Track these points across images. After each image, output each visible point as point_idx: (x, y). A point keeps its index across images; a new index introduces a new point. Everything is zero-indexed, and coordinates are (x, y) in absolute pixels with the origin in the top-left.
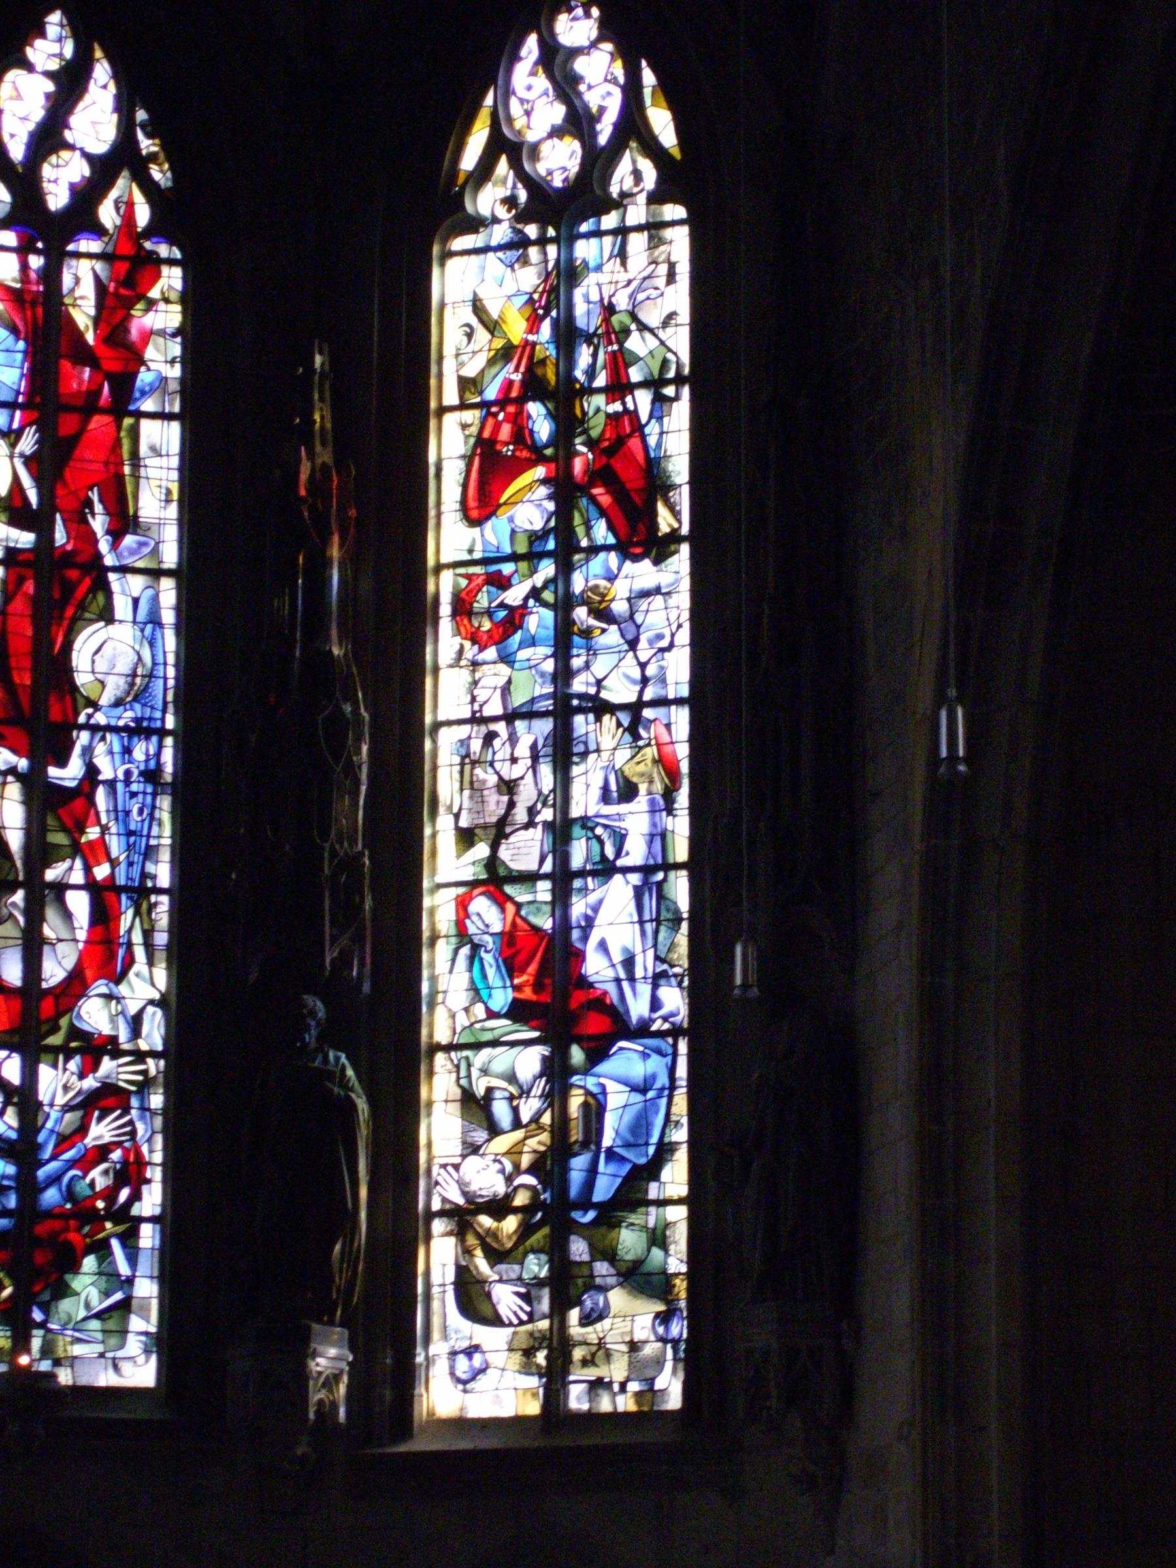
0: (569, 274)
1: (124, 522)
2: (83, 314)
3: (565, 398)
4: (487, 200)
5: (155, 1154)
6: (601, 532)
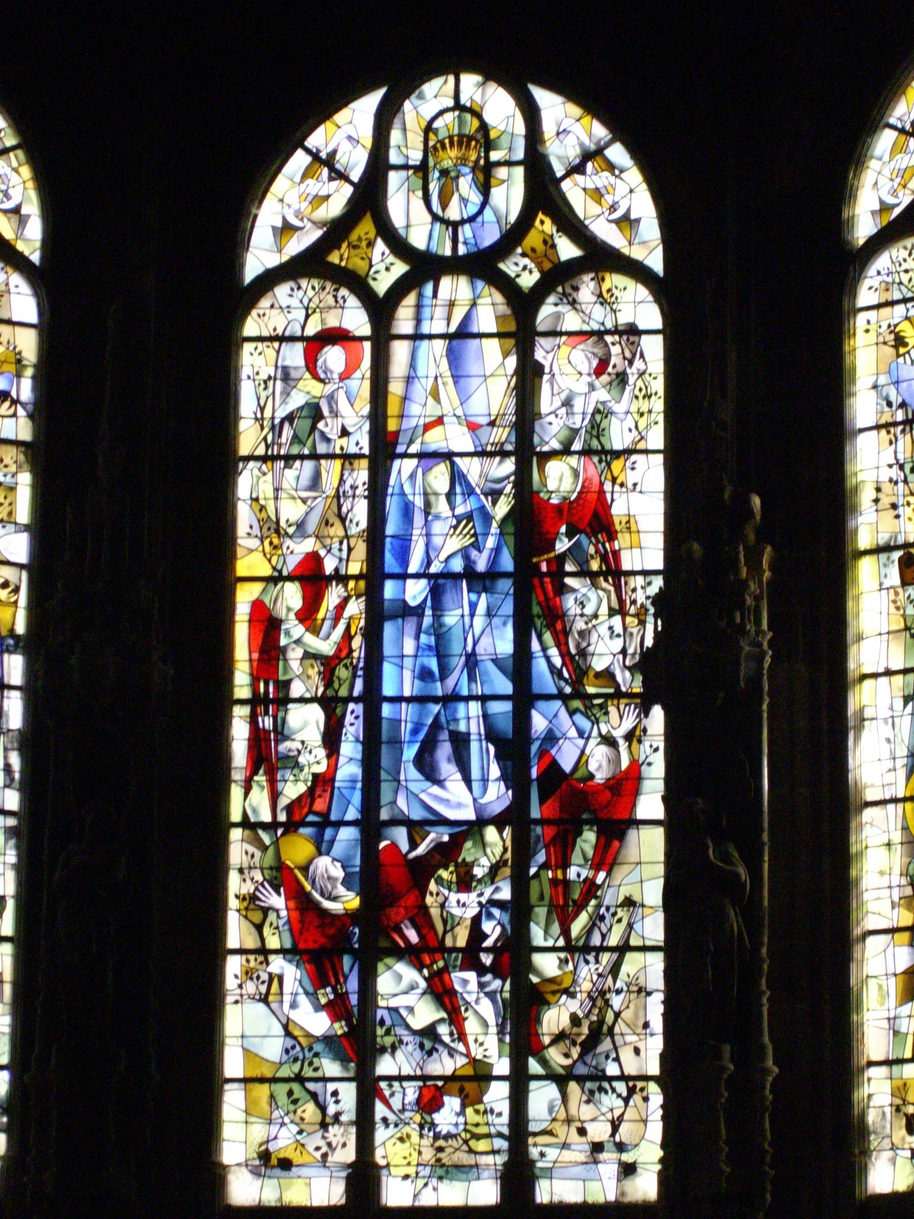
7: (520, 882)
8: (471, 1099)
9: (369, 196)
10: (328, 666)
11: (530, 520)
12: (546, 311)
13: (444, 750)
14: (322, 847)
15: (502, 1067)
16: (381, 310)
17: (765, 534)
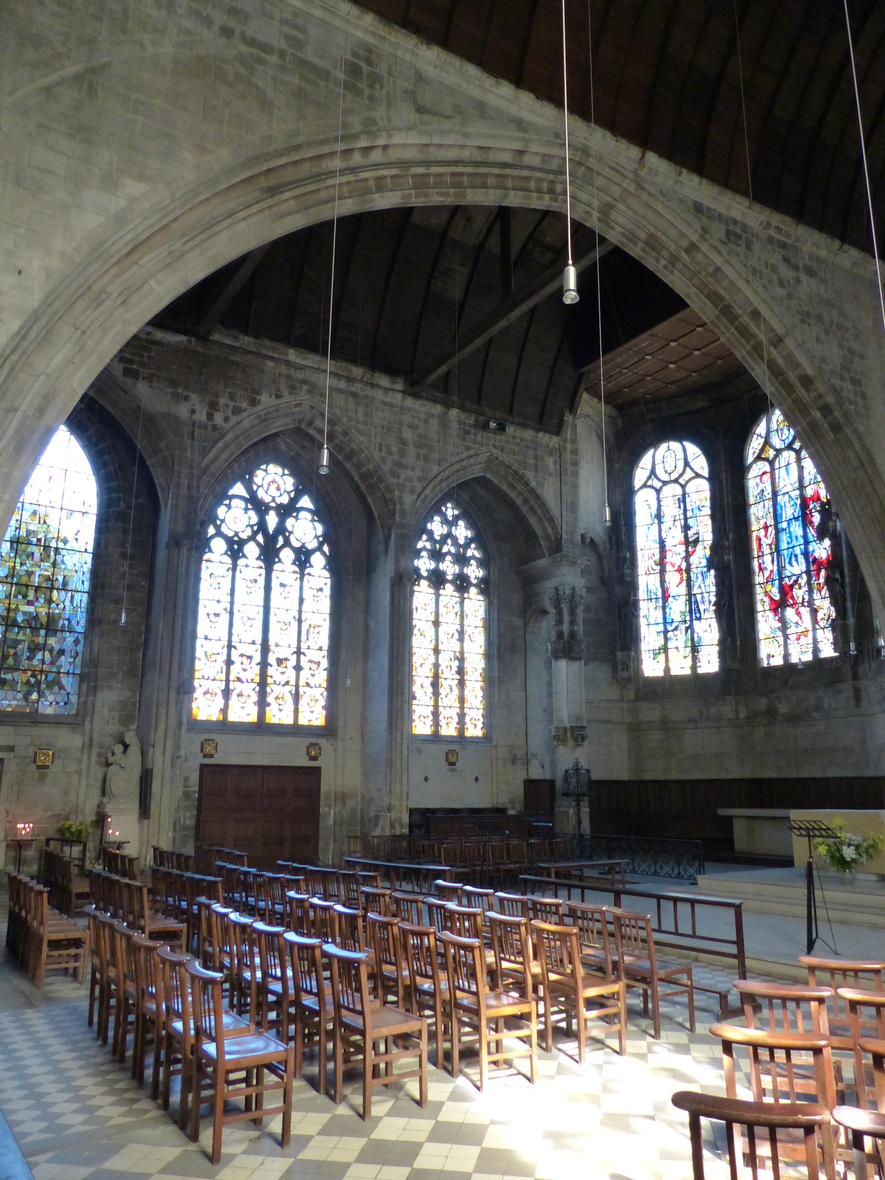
8: (806, 636)
10: (770, 545)
14: (773, 585)
15: (810, 628)
16: (772, 463)
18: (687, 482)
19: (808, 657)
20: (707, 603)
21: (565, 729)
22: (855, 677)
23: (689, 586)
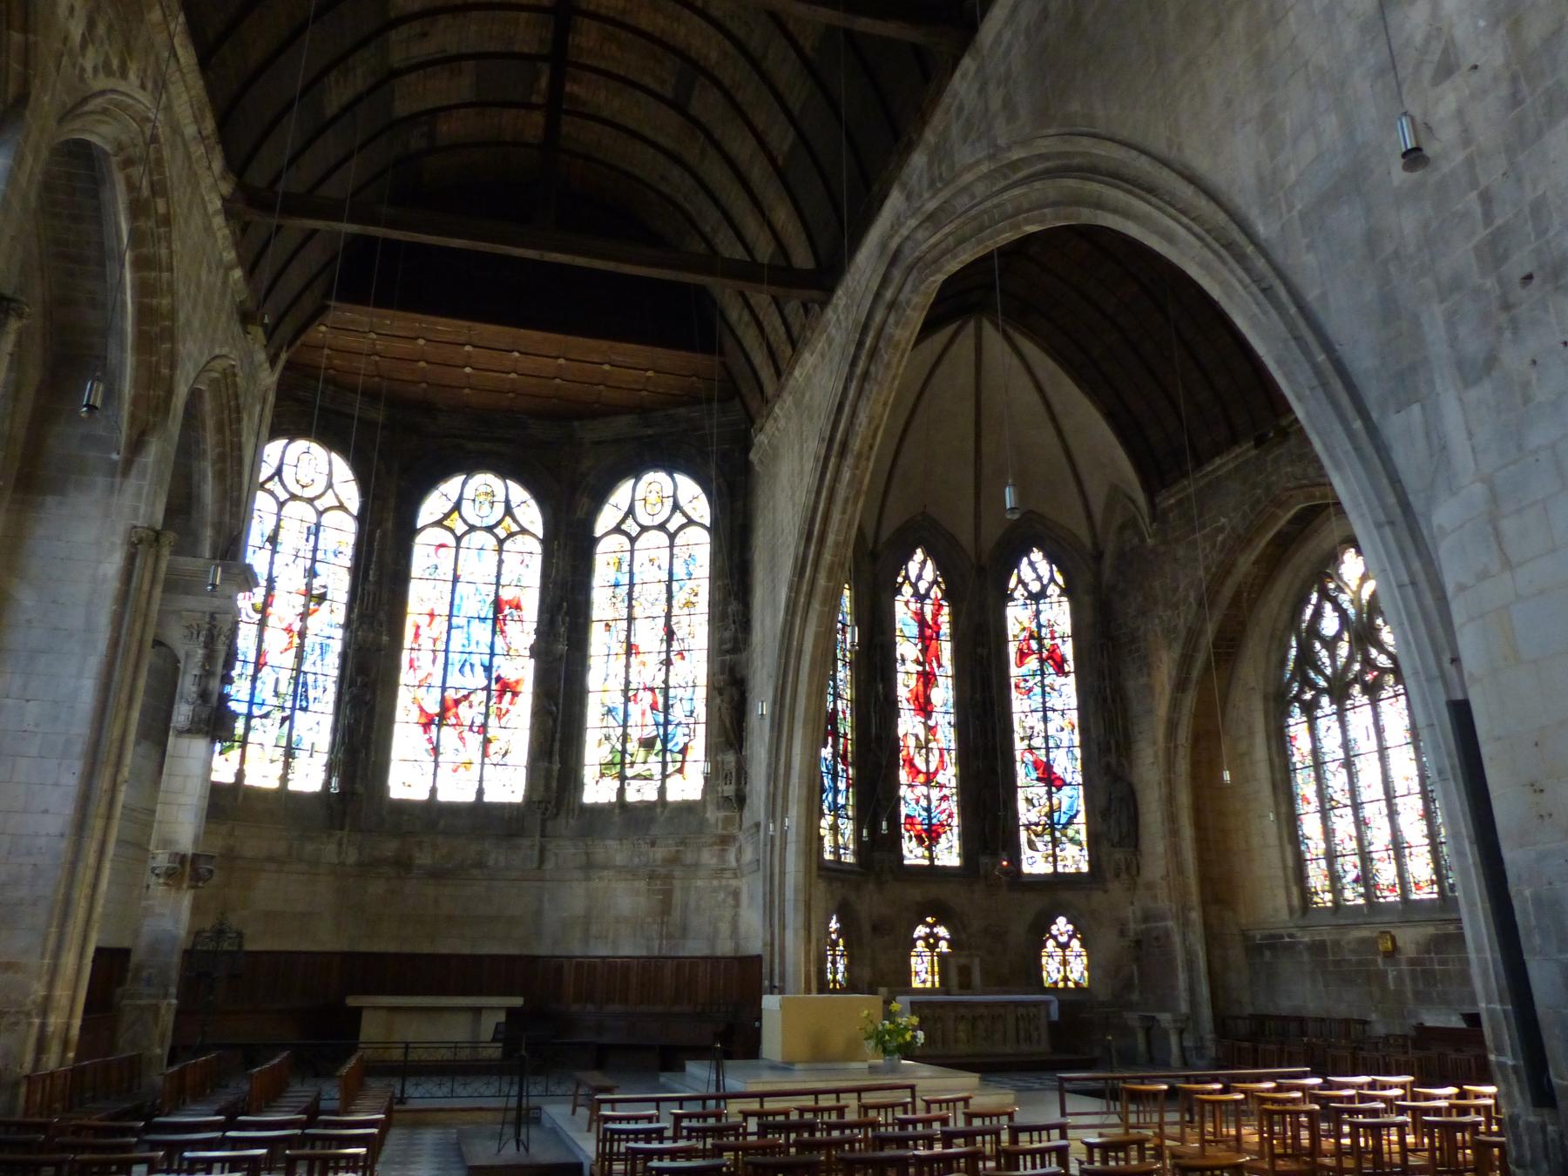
0: (1038, 613)
1: (940, 665)
2: (929, 617)
3: (1040, 639)
4: (1017, 594)
5: (955, 810)
6: (1051, 670)
7: (487, 707)
9: (457, 507)
11: (498, 605)
12: (507, 546)
13: (467, 667)
15: (477, 758)
16: (458, 539)
17: (567, 614)
18: (326, 510)
19: (469, 797)
20: (320, 690)
21: (183, 858)
22: (543, 836)
23: (300, 656)
